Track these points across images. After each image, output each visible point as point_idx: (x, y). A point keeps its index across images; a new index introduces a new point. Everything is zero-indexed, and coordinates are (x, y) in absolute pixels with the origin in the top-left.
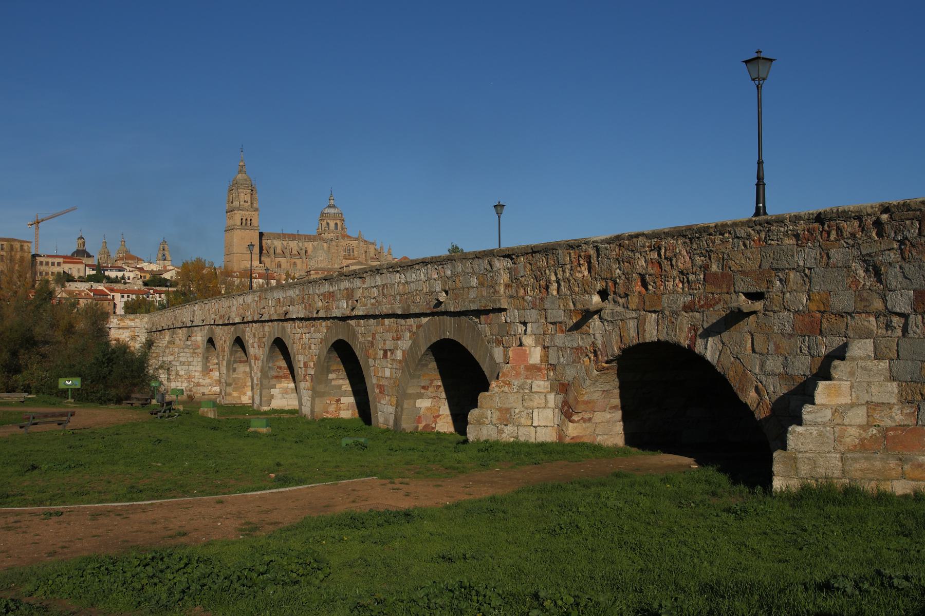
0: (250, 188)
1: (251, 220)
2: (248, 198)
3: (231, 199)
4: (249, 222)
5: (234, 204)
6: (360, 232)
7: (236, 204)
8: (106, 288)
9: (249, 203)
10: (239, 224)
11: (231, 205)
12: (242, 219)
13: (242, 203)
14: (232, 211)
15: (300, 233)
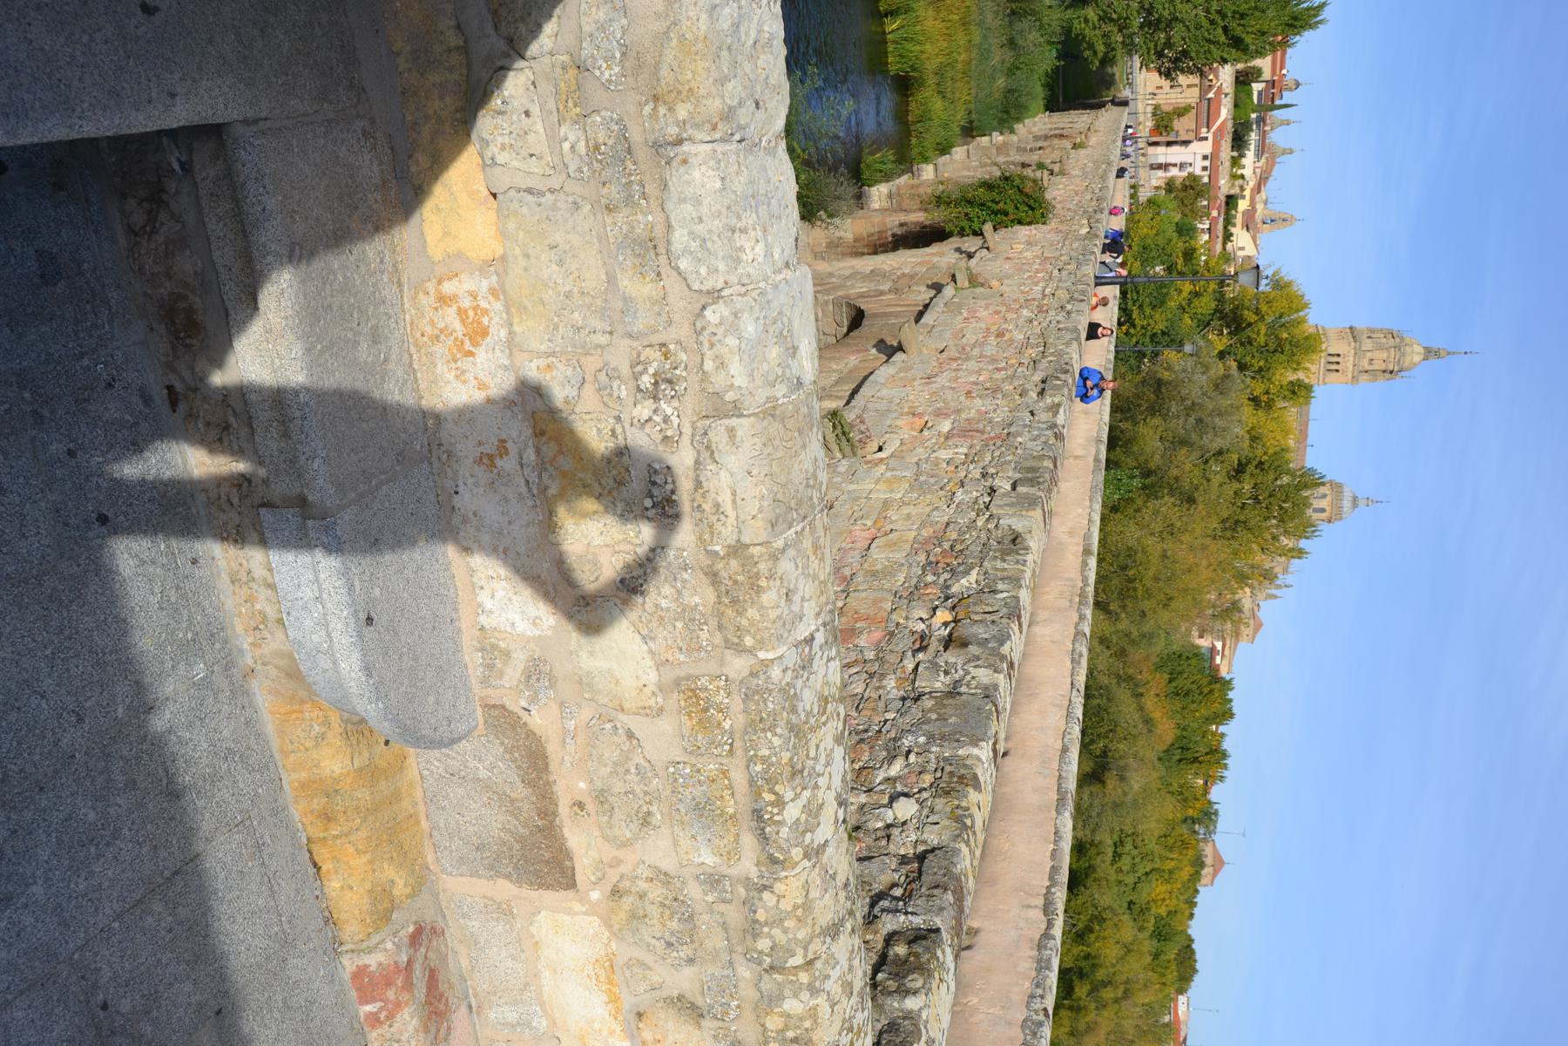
0: (1396, 369)
1: (1337, 371)
2: (1378, 365)
3: (1378, 335)
4: (1334, 367)
5: (1369, 341)
7: (1368, 344)
8: (1223, 123)
9: (1367, 367)
11: (1365, 336)
12: (1339, 355)
13: (1369, 354)
14: (1354, 337)
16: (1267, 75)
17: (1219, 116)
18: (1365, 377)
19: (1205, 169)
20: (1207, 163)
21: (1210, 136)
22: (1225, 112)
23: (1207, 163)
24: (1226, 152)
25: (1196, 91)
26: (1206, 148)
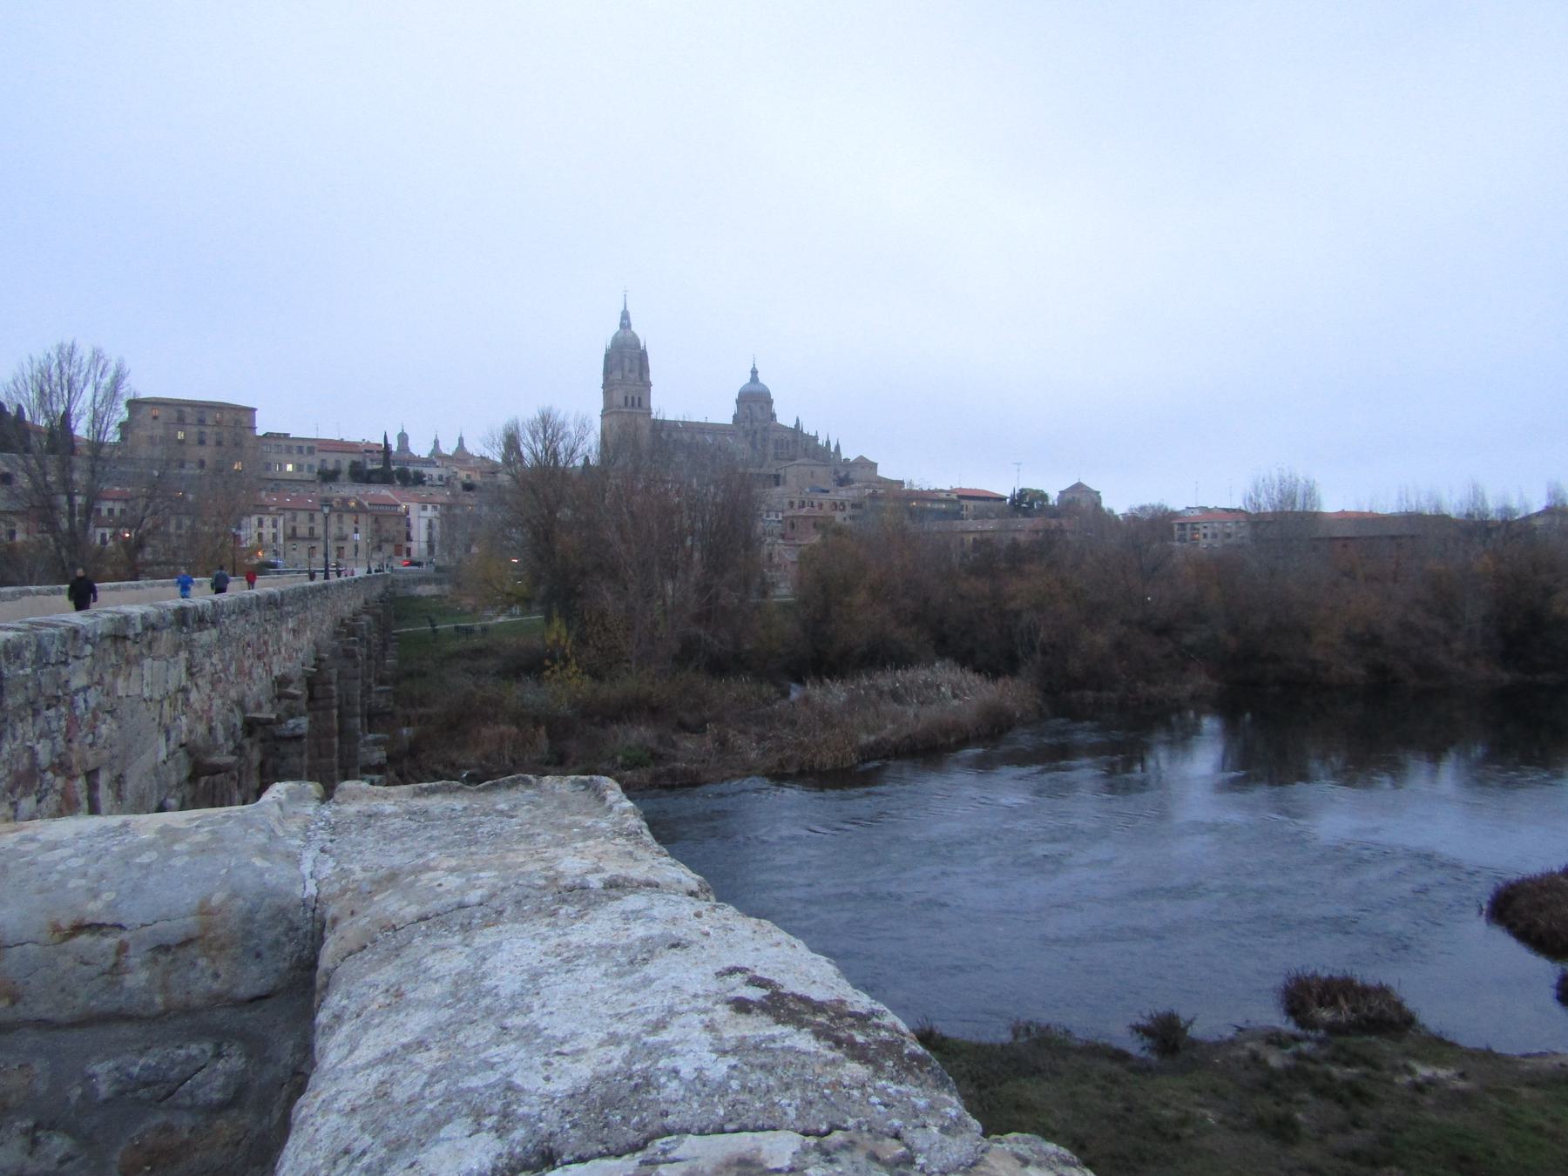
1: (639, 399)
6: (798, 420)
7: (617, 375)
9: (637, 374)
10: (622, 402)
12: (626, 398)
15: (709, 421)
16: (356, 458)
17: (388, 496)
18: (644, 375)
19: (435, 508)
20: (429, 507)
21: (408, 504)
22: (385, 492)
23: (429, 507)
24: (423, 492)
25: (362, 518)
26: (414, 508)
